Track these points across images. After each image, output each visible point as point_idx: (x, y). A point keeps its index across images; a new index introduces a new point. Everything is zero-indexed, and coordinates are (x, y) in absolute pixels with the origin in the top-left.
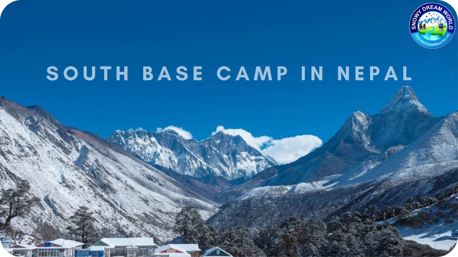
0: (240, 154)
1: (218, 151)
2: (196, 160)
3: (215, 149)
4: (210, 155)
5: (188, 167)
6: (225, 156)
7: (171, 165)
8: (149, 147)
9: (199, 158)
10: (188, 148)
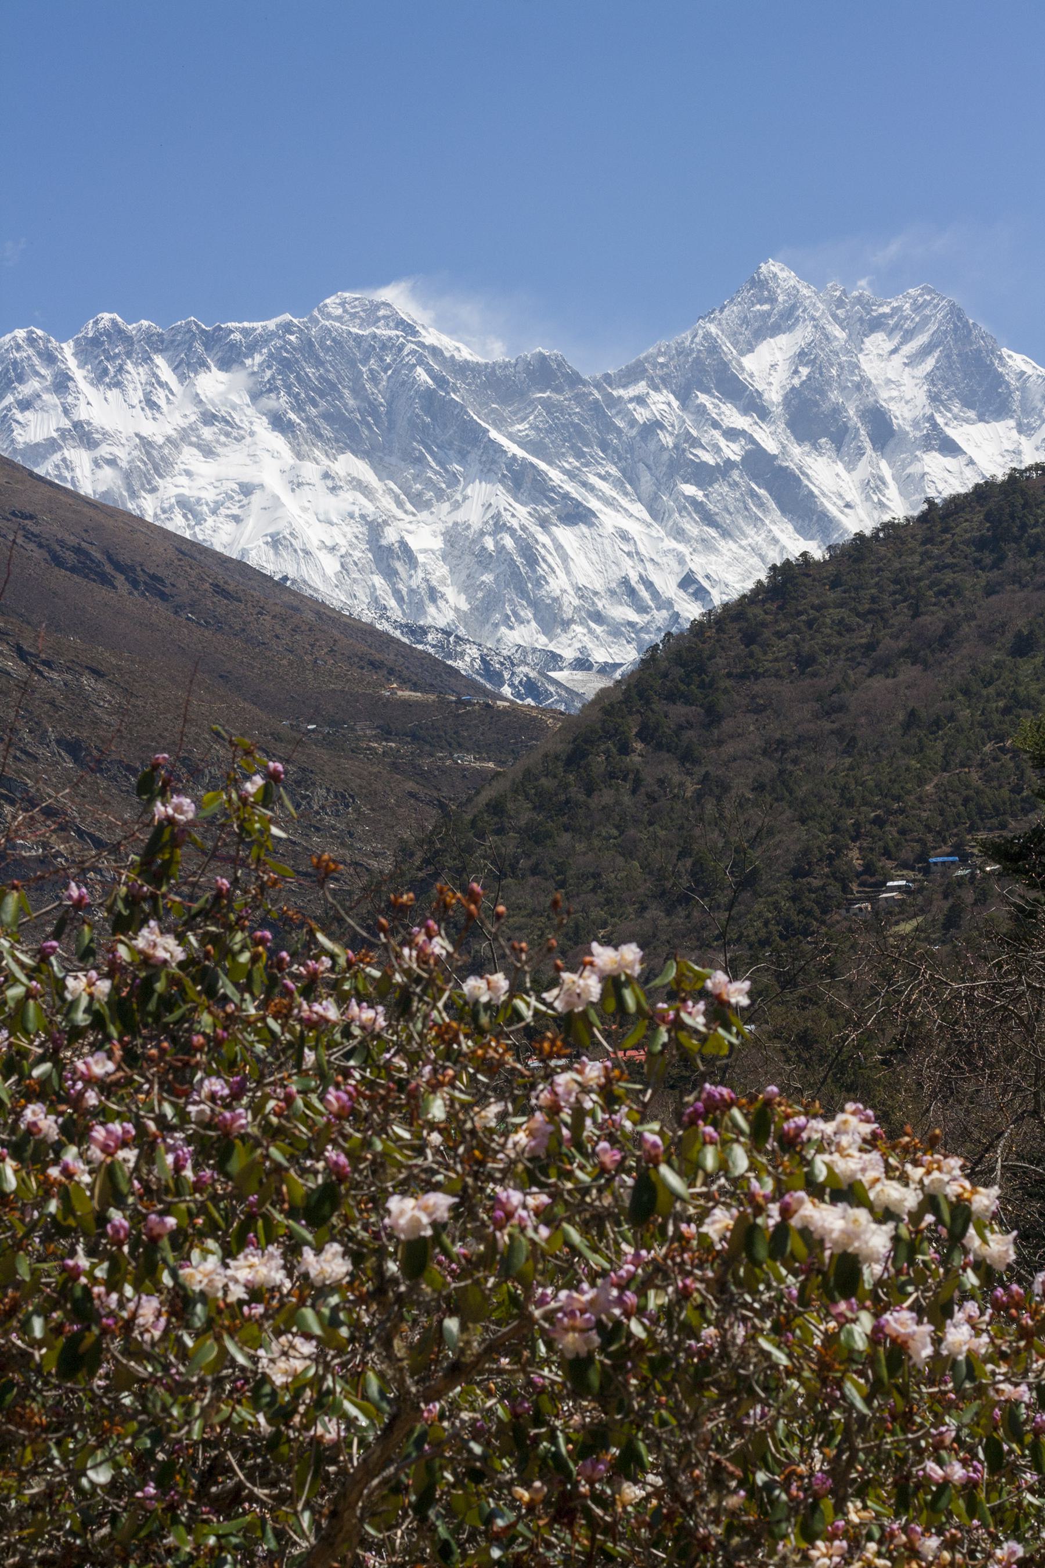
4: (703, 475)
5: (523, 593)
7: (378, 580)
8: (189, 457)
9: (609, 502)
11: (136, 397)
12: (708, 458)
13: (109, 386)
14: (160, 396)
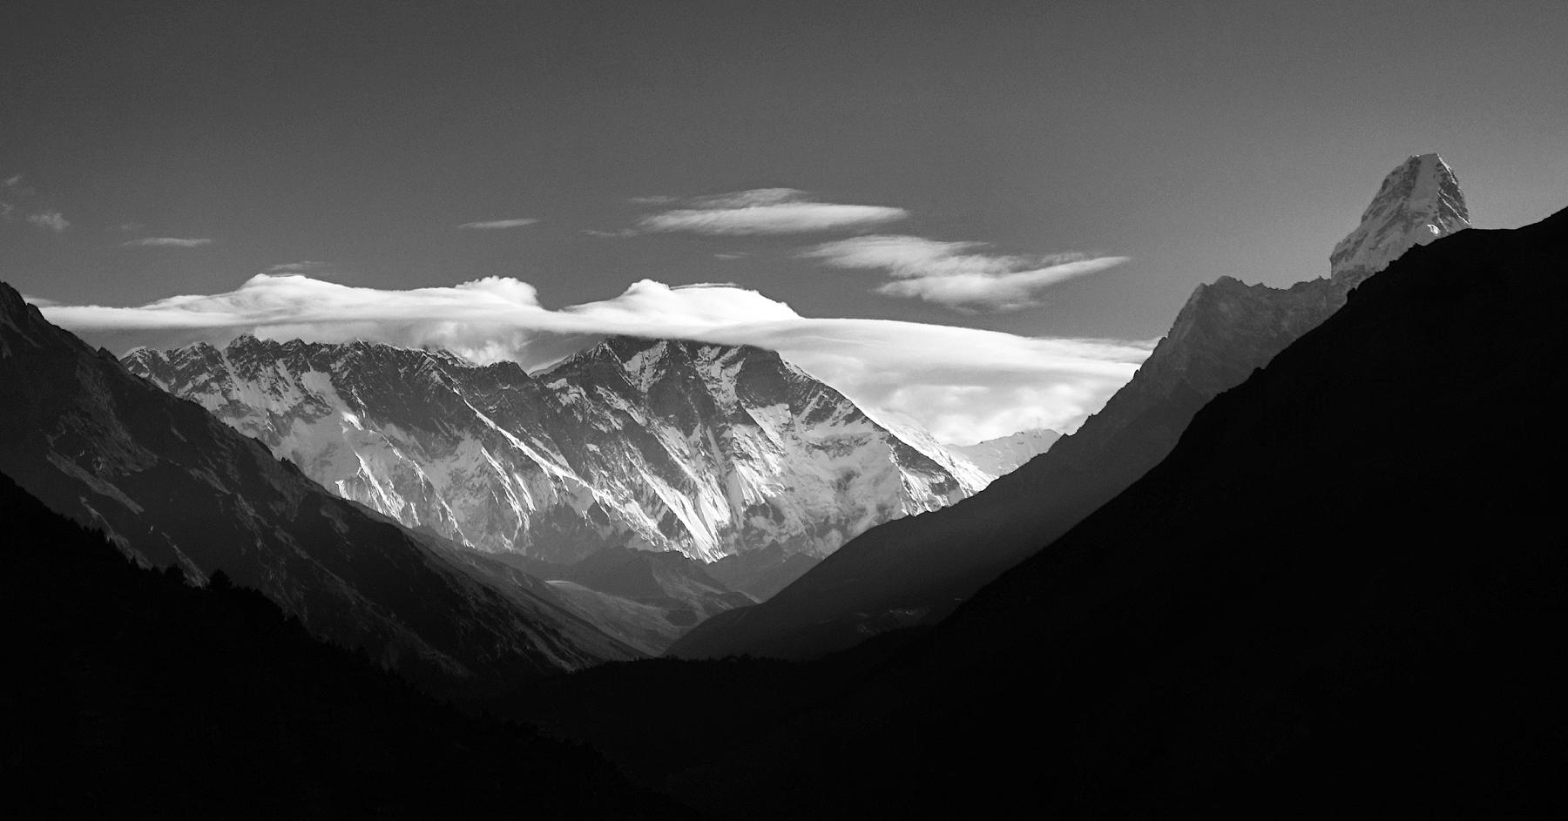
0: (749, 421)
1: (635, 415)
2: (528, 467)
3: (622, 405)
4: (598, 438)
6: (672, 440)
10: (486, 414)
11: (266, 386)
12: (604, 429)
13: (250, 379)
14: (280, 386)
